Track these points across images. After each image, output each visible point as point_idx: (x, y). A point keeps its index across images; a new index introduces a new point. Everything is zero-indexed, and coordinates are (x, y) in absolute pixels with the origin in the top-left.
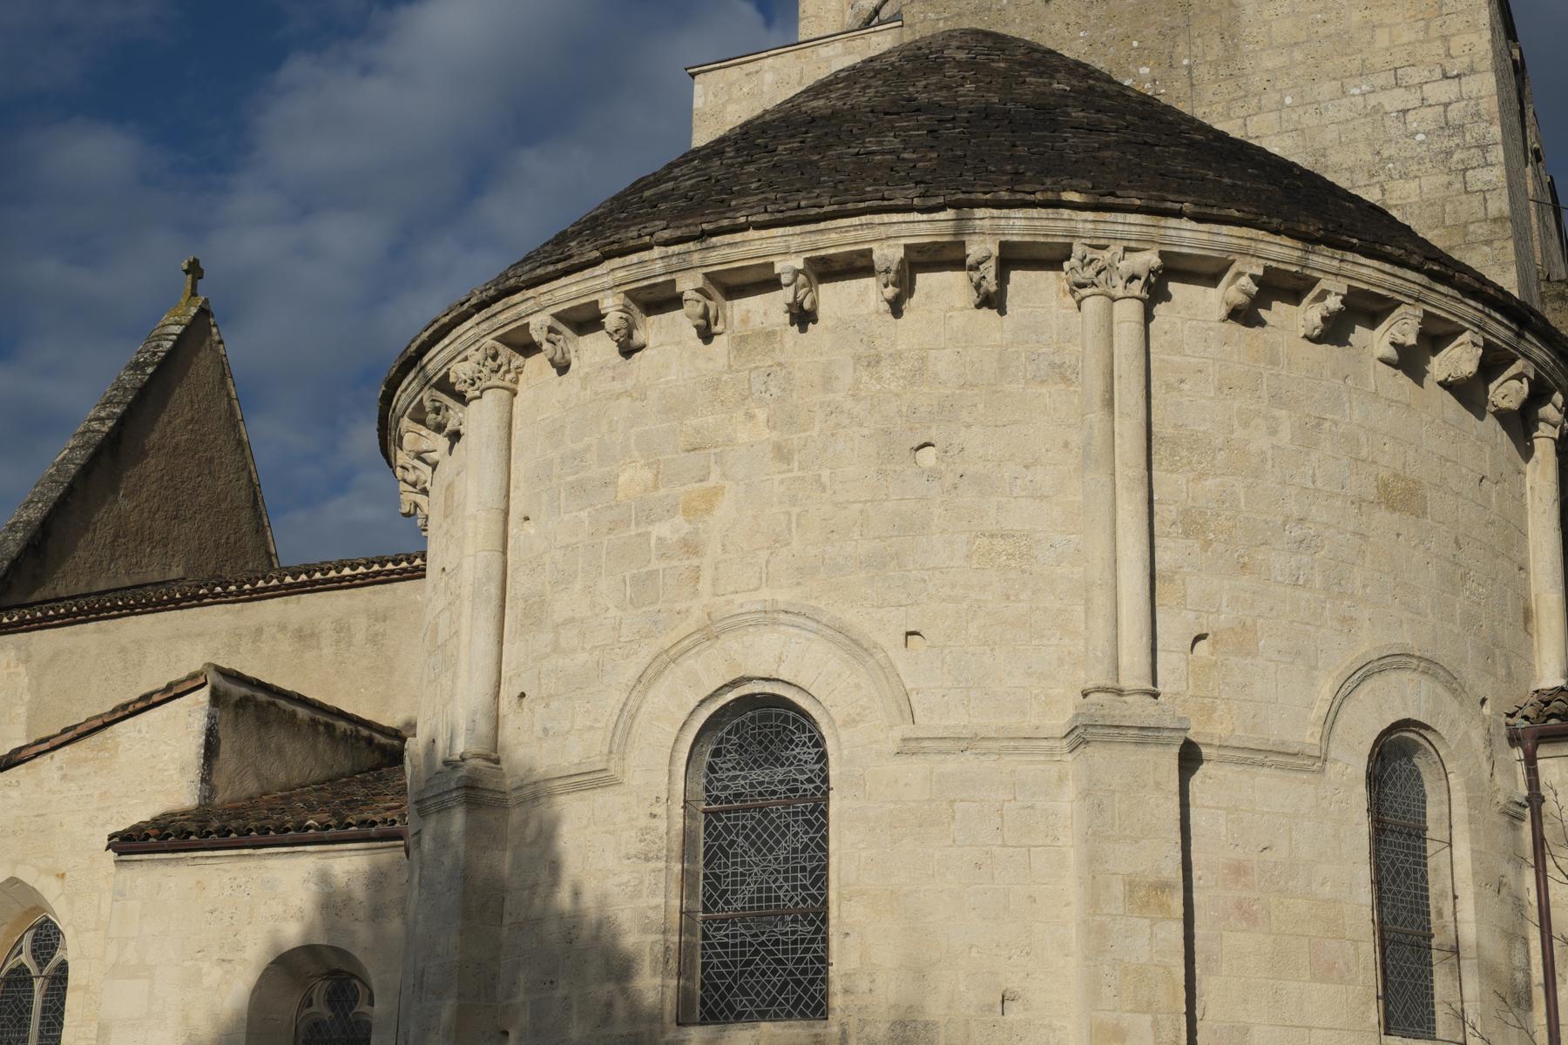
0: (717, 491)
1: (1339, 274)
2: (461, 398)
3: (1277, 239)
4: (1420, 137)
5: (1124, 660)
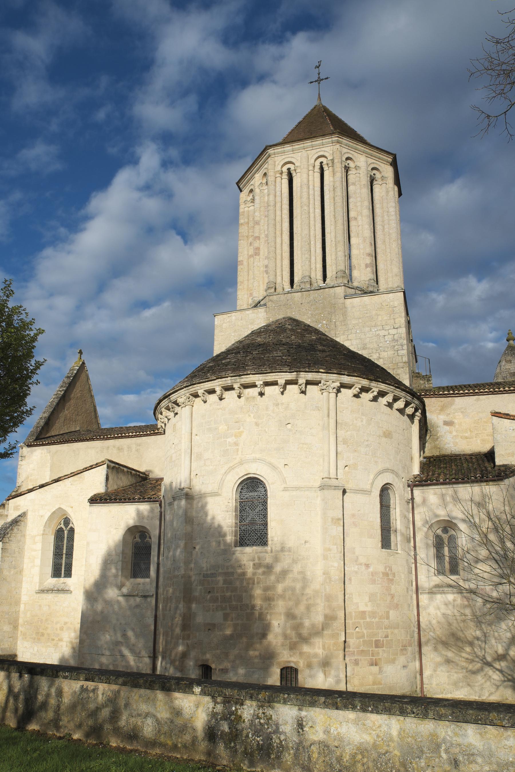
0: (242, 432)
1: (377, 387)
2: (178, 405)
3: (364, 380)
4: (388, 342)
5: (331, 471)
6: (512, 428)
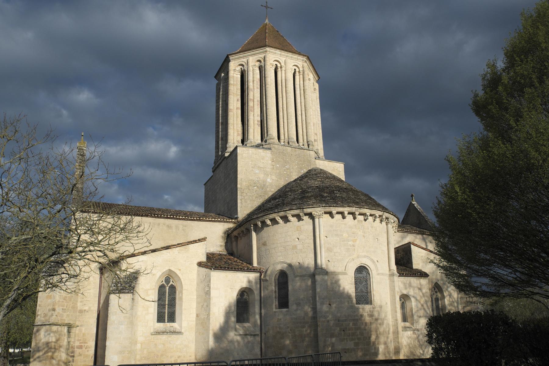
0: (357, 239)
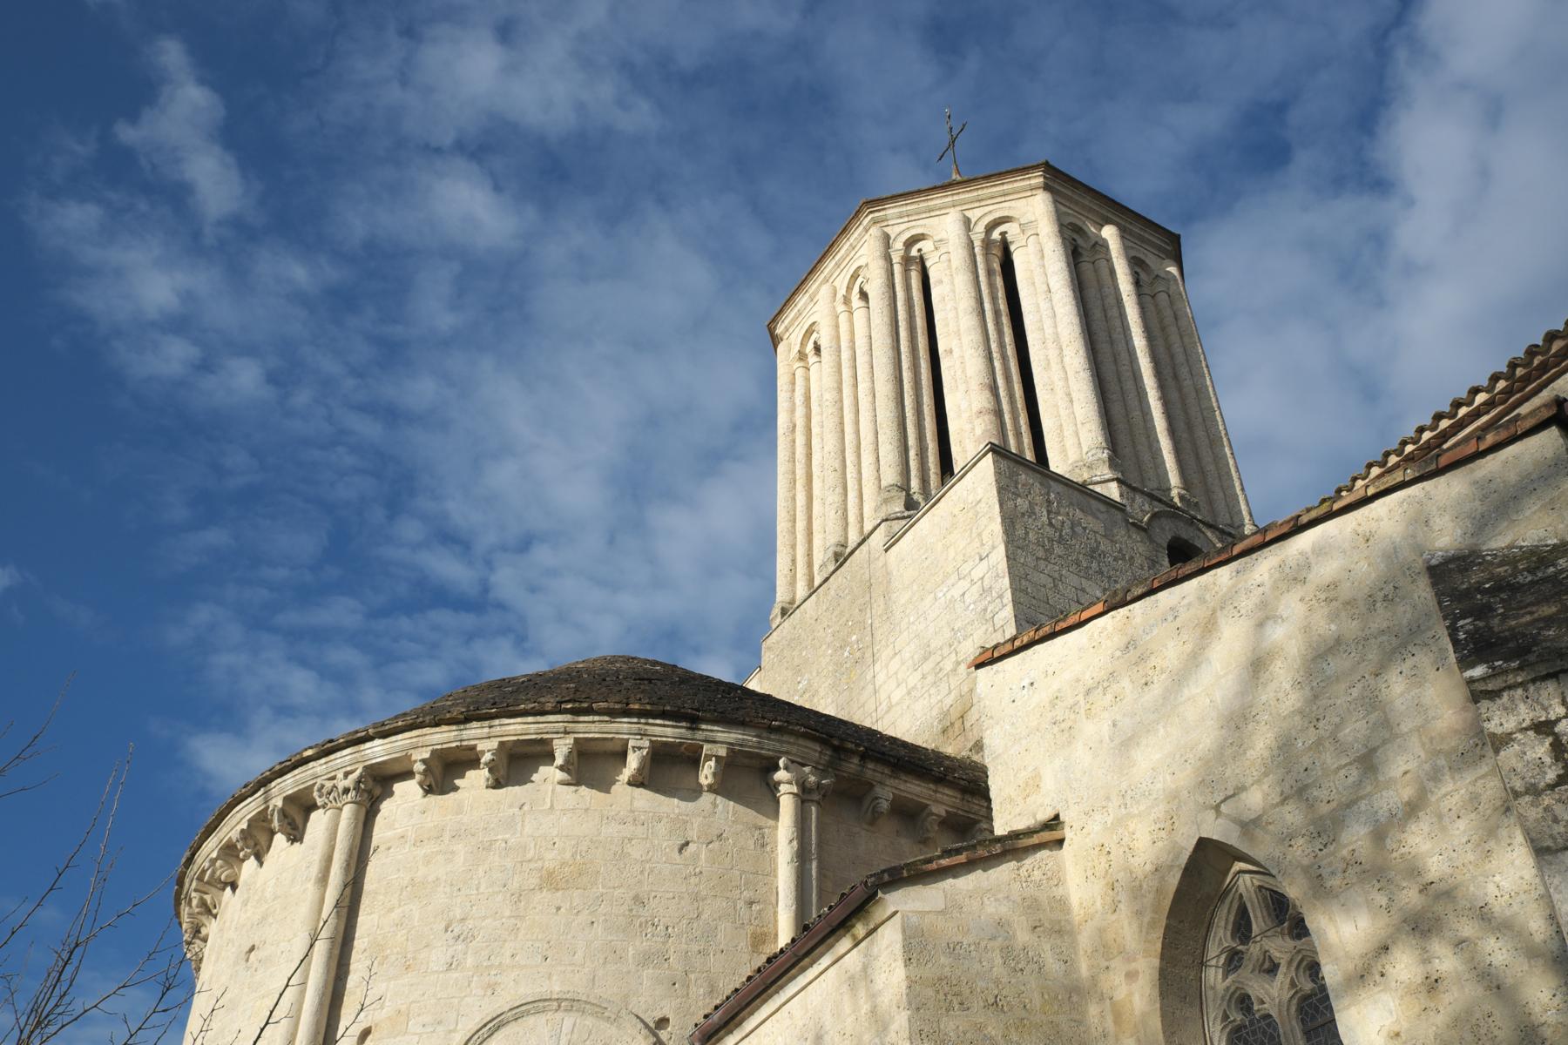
6: (1026, 683)
